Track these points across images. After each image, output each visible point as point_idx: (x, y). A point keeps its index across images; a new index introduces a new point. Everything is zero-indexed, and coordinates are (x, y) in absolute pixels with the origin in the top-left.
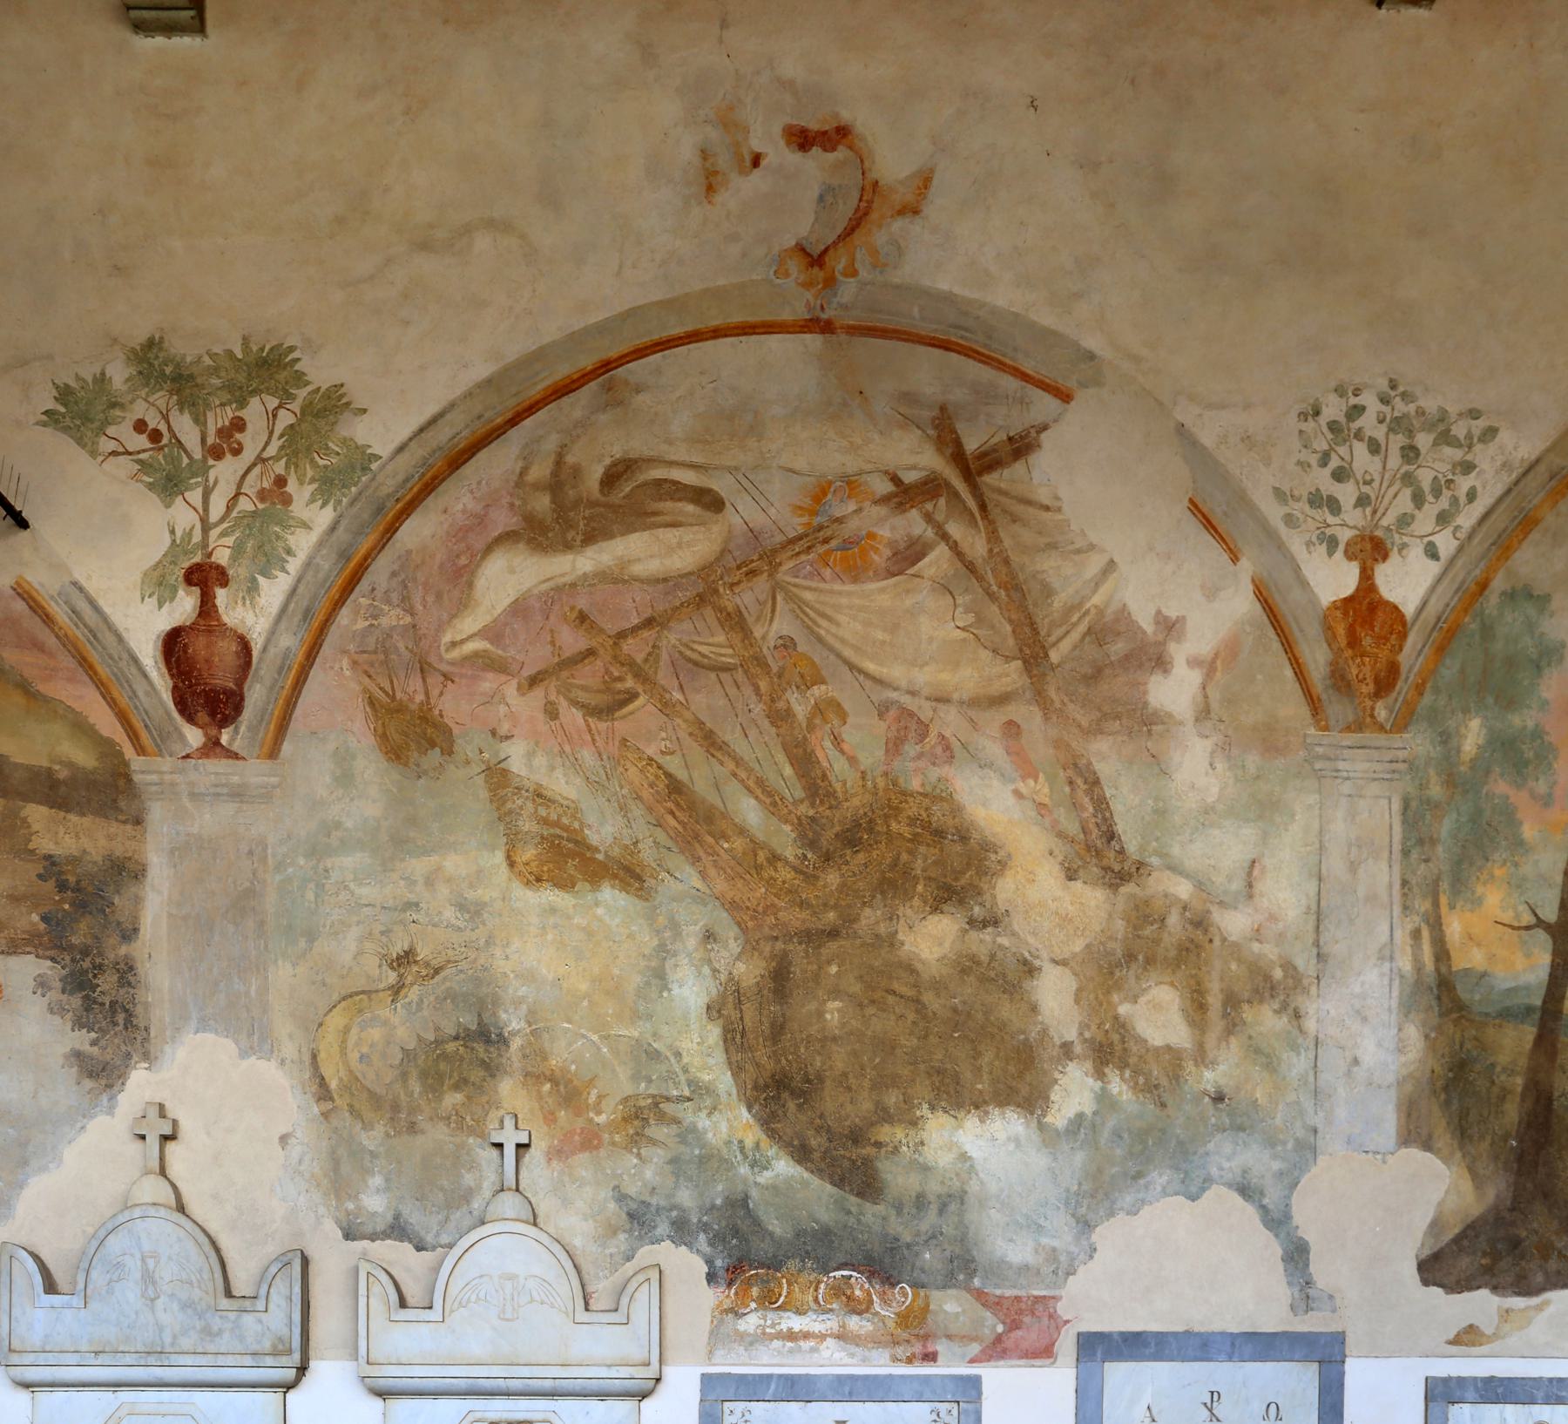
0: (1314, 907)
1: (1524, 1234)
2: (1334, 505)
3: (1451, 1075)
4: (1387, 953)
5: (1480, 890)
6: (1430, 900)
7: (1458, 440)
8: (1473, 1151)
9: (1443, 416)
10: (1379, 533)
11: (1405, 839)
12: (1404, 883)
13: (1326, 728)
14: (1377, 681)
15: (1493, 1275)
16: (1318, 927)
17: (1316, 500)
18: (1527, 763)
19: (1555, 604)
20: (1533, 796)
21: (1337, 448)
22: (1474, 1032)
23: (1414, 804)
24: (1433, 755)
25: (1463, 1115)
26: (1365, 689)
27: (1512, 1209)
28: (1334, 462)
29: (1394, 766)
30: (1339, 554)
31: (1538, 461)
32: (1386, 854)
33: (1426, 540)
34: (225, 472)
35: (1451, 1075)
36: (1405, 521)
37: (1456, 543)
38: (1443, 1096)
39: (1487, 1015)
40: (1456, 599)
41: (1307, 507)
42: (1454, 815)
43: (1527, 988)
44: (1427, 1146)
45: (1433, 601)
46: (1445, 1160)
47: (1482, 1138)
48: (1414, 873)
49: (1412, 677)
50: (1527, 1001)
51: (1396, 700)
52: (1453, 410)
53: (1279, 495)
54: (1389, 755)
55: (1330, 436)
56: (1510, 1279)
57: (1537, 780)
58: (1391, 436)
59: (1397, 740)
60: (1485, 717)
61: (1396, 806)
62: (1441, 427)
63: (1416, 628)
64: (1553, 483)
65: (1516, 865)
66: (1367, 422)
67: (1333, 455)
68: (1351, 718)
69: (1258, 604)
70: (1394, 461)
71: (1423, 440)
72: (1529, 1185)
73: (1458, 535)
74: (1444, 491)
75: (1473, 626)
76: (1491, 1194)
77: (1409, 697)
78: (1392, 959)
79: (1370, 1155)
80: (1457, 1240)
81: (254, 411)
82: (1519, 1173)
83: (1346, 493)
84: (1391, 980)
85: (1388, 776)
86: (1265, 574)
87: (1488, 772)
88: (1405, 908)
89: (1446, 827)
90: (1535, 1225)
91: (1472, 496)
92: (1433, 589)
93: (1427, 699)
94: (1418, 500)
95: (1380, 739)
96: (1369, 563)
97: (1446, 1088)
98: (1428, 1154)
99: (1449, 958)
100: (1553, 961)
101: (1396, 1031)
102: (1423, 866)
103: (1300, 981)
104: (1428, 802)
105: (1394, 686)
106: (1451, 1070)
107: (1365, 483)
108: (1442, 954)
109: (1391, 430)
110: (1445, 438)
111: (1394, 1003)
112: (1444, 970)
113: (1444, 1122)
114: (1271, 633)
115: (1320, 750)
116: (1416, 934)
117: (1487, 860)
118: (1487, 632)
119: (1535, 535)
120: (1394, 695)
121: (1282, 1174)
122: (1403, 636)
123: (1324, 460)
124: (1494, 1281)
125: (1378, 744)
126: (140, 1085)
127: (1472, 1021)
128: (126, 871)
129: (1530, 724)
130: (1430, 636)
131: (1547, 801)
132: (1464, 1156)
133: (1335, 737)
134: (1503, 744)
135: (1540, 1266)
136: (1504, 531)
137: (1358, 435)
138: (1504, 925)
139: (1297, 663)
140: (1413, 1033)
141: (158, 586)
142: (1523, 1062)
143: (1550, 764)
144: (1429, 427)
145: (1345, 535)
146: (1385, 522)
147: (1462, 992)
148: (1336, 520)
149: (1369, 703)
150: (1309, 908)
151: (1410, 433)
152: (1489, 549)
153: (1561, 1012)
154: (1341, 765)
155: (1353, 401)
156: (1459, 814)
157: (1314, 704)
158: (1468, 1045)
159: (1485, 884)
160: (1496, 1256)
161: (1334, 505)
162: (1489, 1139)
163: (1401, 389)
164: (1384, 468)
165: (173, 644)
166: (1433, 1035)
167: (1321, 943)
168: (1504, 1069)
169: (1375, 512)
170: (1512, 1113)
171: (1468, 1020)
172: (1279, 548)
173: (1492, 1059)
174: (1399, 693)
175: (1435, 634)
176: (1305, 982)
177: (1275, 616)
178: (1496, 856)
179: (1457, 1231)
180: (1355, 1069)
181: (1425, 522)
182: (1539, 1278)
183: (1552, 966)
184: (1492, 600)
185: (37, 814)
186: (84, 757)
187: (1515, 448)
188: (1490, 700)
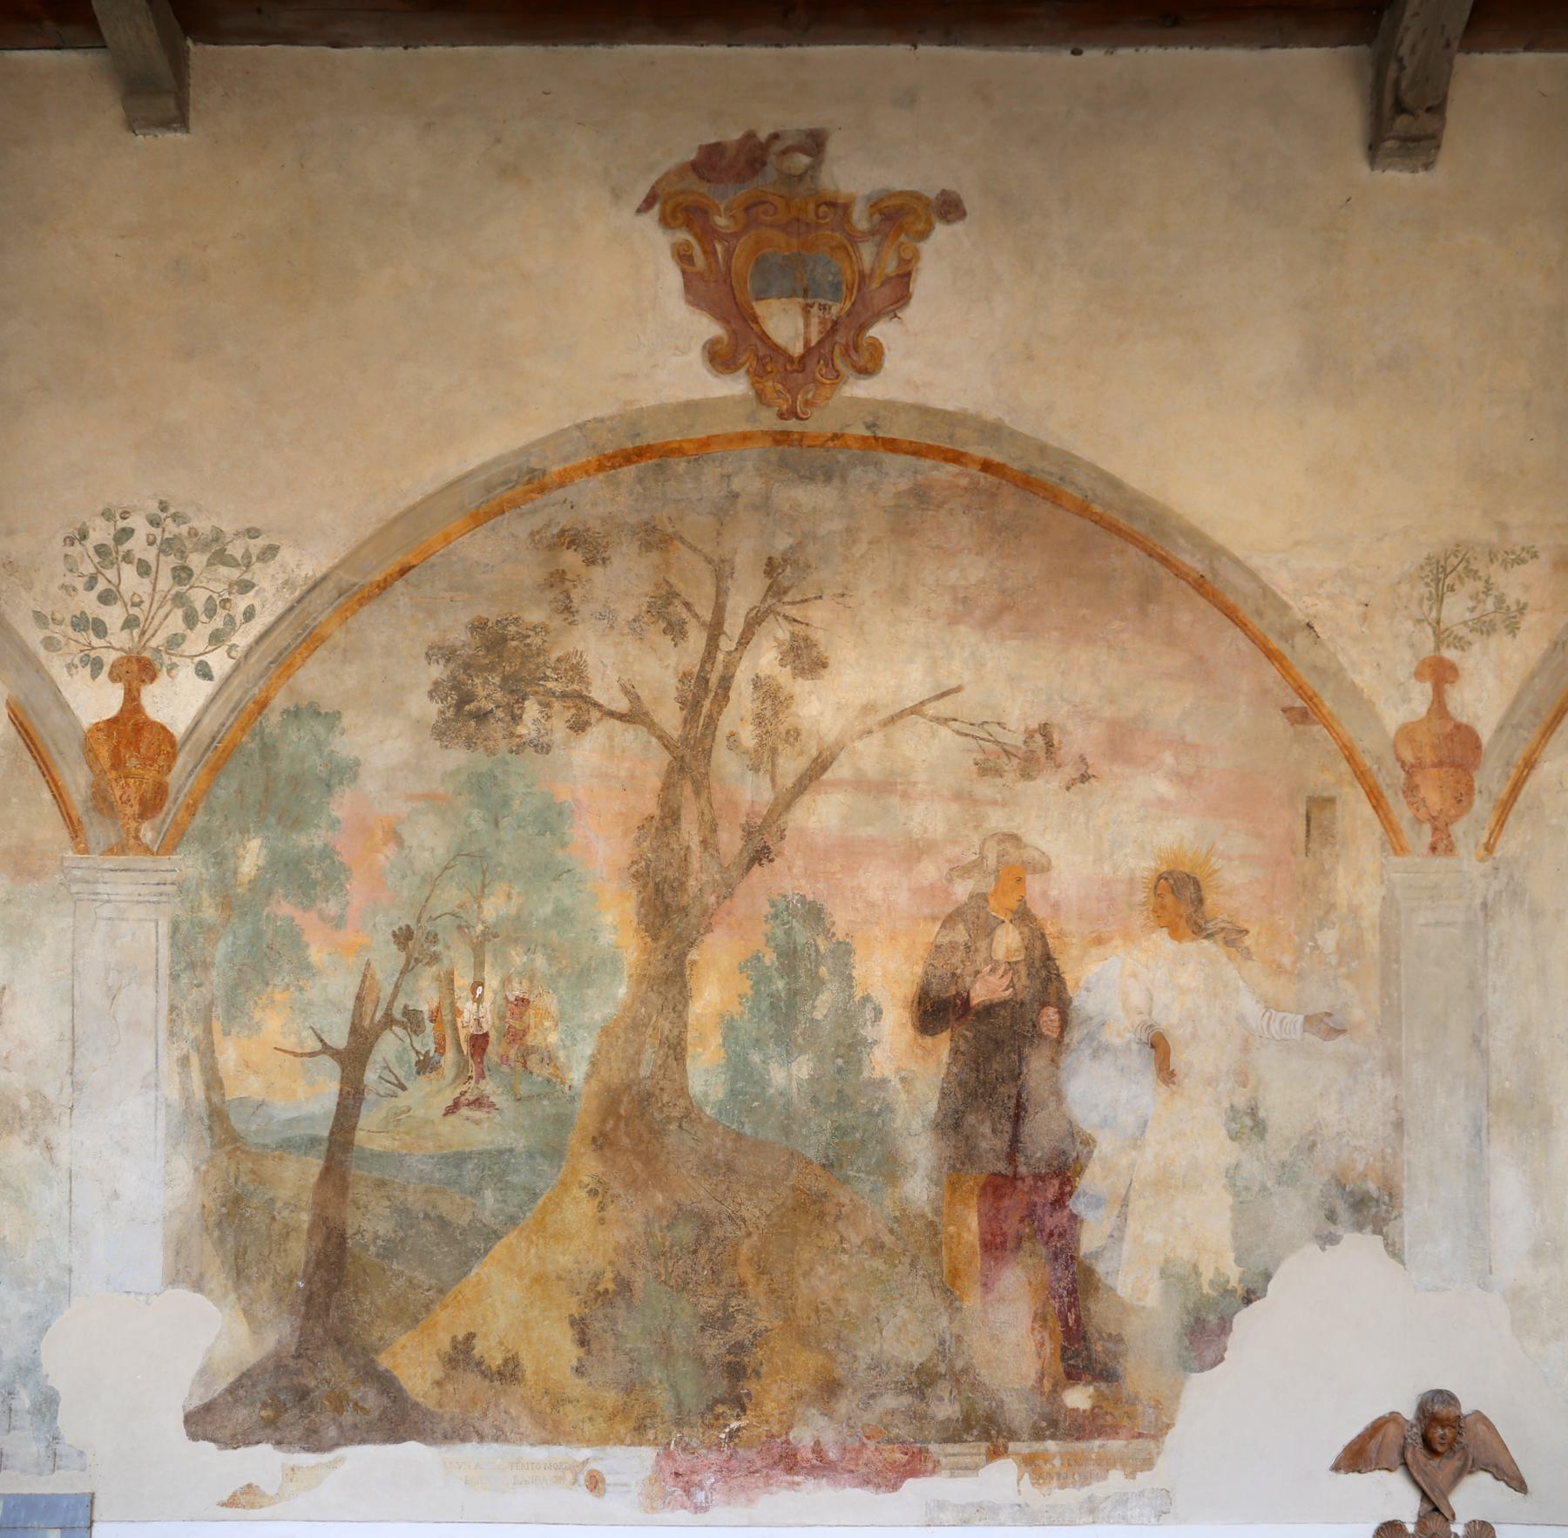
0: (68, 1034)
1: (313, 1383)
2: (100, 628)
3: (224, 1210)
5: (258, 1015)
6: (201, 1025)
7: (235, 559)
8: (251, 1292)
9: (218, 535)
10: (147, 654)
11: (173, 963)
12: (173, 1009)
13: (86, 851)
14: (142, 802)
15: (277, 1429)
16: (74, 1054)
17: (80, 622)
18: (315, 884)
19: (346, 721)
20: (323, 918)
21: (104, 571)
22: (250, 1165)
23: (184, 927)
25: (240, 1253)
26: (129, 811)
27: (299, 1356)
28: (101, 585)
29: (162, 888)
30: (103, 676)
31: (324, 578)
32: (152, 979)
33: (197, 659)
35: (224, 1210)
36: (175, 641)
37: (232, 662)
39: (265, 1146)
40: (232, 718)
41: (70, 631)
42: (231, 938)
43: (311, 1118)
44: (198, 1286)
45: (206, 720)
46: (217, 1302)
47: (262, 1278)
48: (184, 998)
50: (310, 1132)
51: (164, 821)
52: (228, 529)
53: (39, 618)
54: (157, 878)
55: (97, 559)
56: (297, 1434)
57: (327, 901)
58: (162, 557)
59: (164, 862)
60: (267, 838)
61: (165, 928)
62: (215, 547)
63: (187, 748)
64: (342, 599)
65: (301, 989)
66: (137, 545)
67: (100, 578)
68: (113, 839)
69: (12, 728)
70: (165, 581)
71: (197, 561)
72: (319, 1331)
73: (233, 654)
74: (219, 610)
75: (252, 745)
76: (270, 1341)
77: (179, 817)
79: (132, 1295)
80: (232, 1390)
82: (307, 1316)
83: (113, 616)
85: (155, 899)
87: (270, 894)
88: (172, 1034)
89: (221, 950)
90: (326, 1374)
91: (249, 614)
92: (206, 709)
93: (200, 819)
94: (191, 620)
95: (146, 862)
96: (135, 684)
97: (219, 1224)
98: (198, 1295)
99: (221, 1087)
100: (341, 1090)
101: (163, 1164)
102: (195, 990)
104: (201, 924)
105: (162, 808)
106: (224, 1205)
107: (134, 605)
108: (213, 1081)
109: (161, 551)
110: (221, 557)
111: (161, 1134)
112: (215, 1099)
113: (218, 1261)
114: (27, 756)
115: (78, 873)
116: (184, 1061)
117: (267, 984)
118: (268, 751)
119: (321, 652)
120: (162, 815)
121: (30, 1317)
122: (173, 757)
123: (91, 583)
124: (278, 1436)
125: (144, 866)
127: (247, 1153)
129: (318, 844)
130: (203, 756)
131: (338, 923)
132: (239, 1299)
133: (95, 859)
134: (286, 865)
135: (334, 1419)
136: (286, 649)
137: (127, 557)
138: (285, 1051)
139: (56, 785)
140: (183, 1167)
142: (307, 1197)
143: (341, 885)
144: (203, 547)
145: (110, 657)
146: (153, 644)
147: (236, 1122)
148: (102, 643)
149: (133, 825)
150: (62, 1034)
151: (183, 554)
152: (268, 668)
153: (352, 1143)
154: (101, 888)
155: (121, 524)
156: (235, 937)
157: (74, 827)
158: (244, 1179)
159: (263, 1009)
160: (280, 1408)
162: (270, 1280)
163: (172, 510)
164: (154, 590)
166: (204, 1168)
167: (76, 1070)
168: (286, 1205)
169: (143, 633)
170: (298, 1252)
171: (243, 1152)
172: (37, 672)
173: (271, 1194)
175: (209, 754)
176: (56, 1112)
178: (278, 980)
179: (231, 1379)
181: (197, 641)
182: (333, 1432)
183: (341, 1095)
184: (273, 718)
187: (298, 566)
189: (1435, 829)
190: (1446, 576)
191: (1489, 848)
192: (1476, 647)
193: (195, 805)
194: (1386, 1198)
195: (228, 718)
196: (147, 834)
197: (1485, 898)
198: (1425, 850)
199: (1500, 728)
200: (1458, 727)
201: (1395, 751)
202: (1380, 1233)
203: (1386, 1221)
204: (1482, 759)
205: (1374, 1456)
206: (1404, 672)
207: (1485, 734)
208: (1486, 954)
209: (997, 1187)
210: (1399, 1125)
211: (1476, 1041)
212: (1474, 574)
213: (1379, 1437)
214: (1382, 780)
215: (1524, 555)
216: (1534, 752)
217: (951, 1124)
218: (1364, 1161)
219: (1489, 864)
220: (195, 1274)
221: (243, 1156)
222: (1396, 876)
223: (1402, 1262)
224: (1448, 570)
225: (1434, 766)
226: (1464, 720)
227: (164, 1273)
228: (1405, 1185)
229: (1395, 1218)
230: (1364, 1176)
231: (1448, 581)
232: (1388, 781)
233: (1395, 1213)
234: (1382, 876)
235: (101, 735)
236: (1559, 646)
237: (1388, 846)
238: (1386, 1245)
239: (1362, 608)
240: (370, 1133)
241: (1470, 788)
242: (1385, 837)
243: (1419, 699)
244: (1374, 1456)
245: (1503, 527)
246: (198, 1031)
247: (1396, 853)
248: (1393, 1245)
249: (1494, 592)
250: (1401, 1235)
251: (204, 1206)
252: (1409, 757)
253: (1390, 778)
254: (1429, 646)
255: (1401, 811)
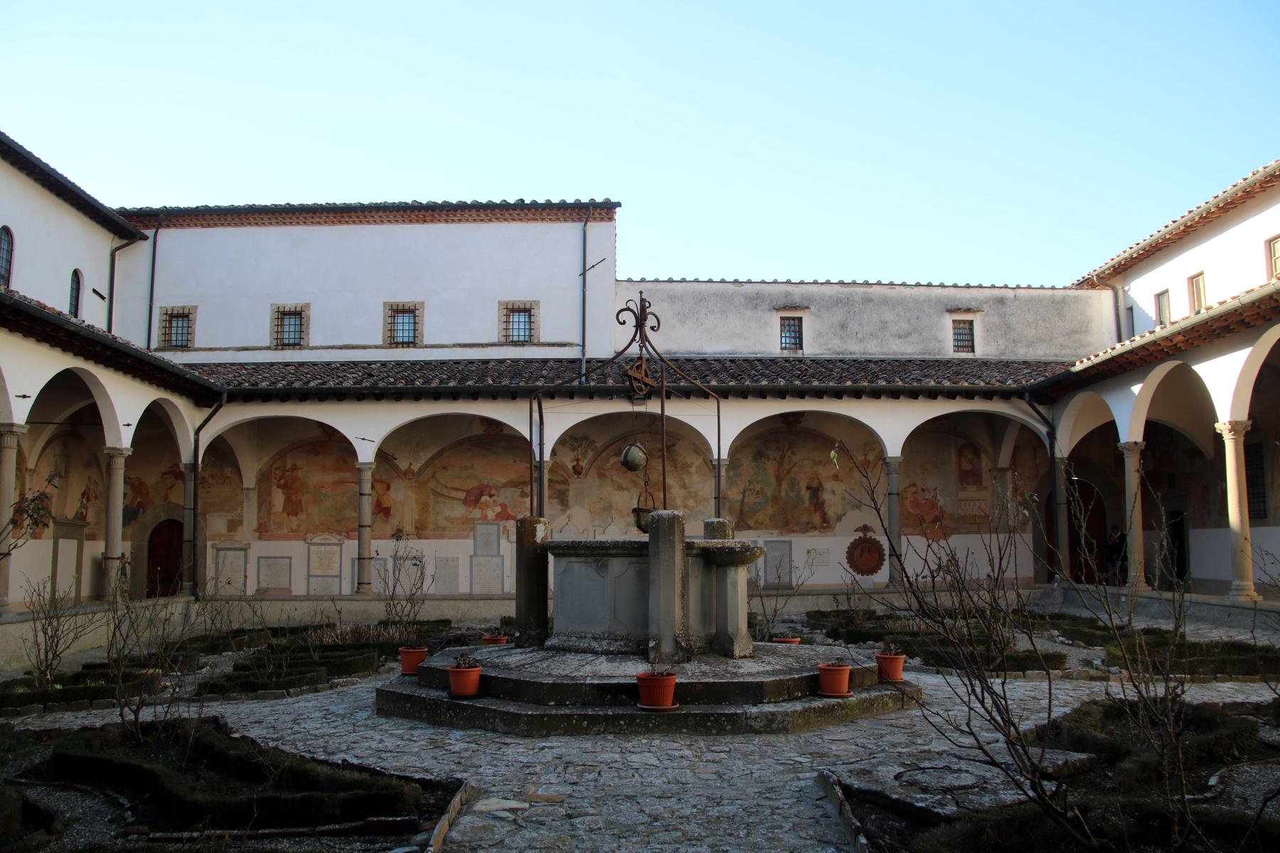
34: (580, 449)
81: (584, 442)
126: (568, 512)
128: (567, 490)
141: (572, 461)
165: (573, 467)
170: (738, 512)
185: (557, 485)
186: (562, 479)
209: (815, 505)
217: (810, 499)
240: (746, 500)
243: (863, 458)
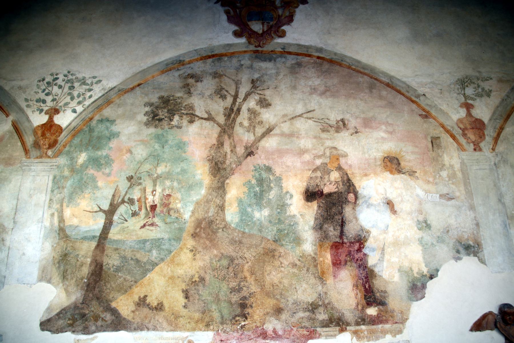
0: (15, 207)
2: (44, 102)
4: (41, 221)
5: (79, 201)
6: (60, 204)
7: (88, 84)
8: (67, 283)
9: (84, 78)
10: (57, 107)
11: (53, 187)
12: (51, 200)
13: (29, 158)
16: (16, 213)
17: (38, 101)
18: (102, 165)
19: (117, 122)
20: (103, 173)
21: (48, 88)
22: (71, 244)
23: (57, 177)
24: (67, 163)
25: (65, 271)
26: (45, 147)
28: (47, 91)
29: (52, 167)
30: (43, 113)
31: (115, 87)
32: (45, 192)
33: (72, 108)
35: (61, 258)
36: (66, 104)
37: (83, 109)
38: (57, 265)
39: (77, 239)
41: (35, 103)
42: (72, 180)
43: (94, 230)
44: (49, 281)
45: (73, 123)
46: (55, 286)
47: (72, 279)
48: (55, 197)
49: (62, 143)
50: (93, 234)
51: (55, 149)
52: (87, 76)
53: (26, 100)
54: (51, 164)
55: (46, 85)
57: (106, 169)
58: (66, 84)
59: (54, 160)
61: (51, 178)
62: (83, 81)
63: (66, 130)
64: (119, 92)
65: (94, 194)
66: (59, 82)
68: (39, 154)
70: (66, 90)
71: (76, 85)
73: (84, 106)
74: (81, 96)
75: (87, 129)
76: (73, 299)
77: (60, 148)
78: (42, 222)
80: (58, 314)
83: (49, 99)
84: (41, 229)
85: (49, 170)
86: (17, 119)
87: (87, 167)
88: (49, 207)
89: (69, 183)
91: (90, 97)
92: (73, 120)
93: (67, 149)
94: (72, 99)
95: (48, 160)
96: (52, 115)
97: (59, 263)
98: (49, 285)
99: (64, 221)
100: (105, 222)
101: (41, 244)
103: (5, 230)
104: (63, 177)
105: (55, 146)
106: (61, 257)
107: (55, 95)
108: (62, 220)
111: (42, 236)
113: (57, 274)
114: (15, 134)
115: (26, 164)
116: (53, 215)
117: (83, 192)
118: (91, 130)
119: (112, 105)
120: (55, 148)
122: (61, 133)
125: (47, 161)
127: (71, 241)
129: (104, 154)
131: (109, 175)
132: (63, 285)
133: (32, 160)
134: (93, 160)
136: (101, 105)
138: (87, 211)
140: (48, 246)
142: (90, 254)
143: (111, 165)
145: (45, 109)
147: (68, 232)
148: (44, 105)
149: (45, 150)
150: (13, 208)
151: (73, 83)
152: (94, 109)
153: (107, 237)
154: (32, 167)
155: (55, 76)
156: (74, 180)
158: (69, 249)
159: (81, 199)
161: (44, 102)
162: (75, 279)
166: (55, 245)
167: (16, 218)
168: (83, 256)
169: (57, 102)
170: (86, 271)
171: (69, 241)
173: (78, 253)
174: (57, 148)
175: (73, 132)
176: (7, 230)
177: (17, 130)
178: (87, 191)
179: (58, 311)
180: (23, 256)
181: (73, 104)
183: (105, 223)
184: (94, 123)
187: (107, 85)
188: (90, 148)
189: (474, 145)
190: (465, 83)
191: (493, 149)
192: (478, 100)
193: (66, 145)
194: (477, 246)
195: (80, 122)
196: (50, 153)
197: (495, 162)
198: (472, 150)
199: (490, 120)
200: (477, 119)
201: (457, 125)
202: (476, 256)
203: (478, 253)
204: (486, 127)
205: (485, 326)
206: (456, 106)
207: (486, 121)
208: (498, 177)
209: (336, 246)
210: (477, 225)
211: (500, 200)
212: (474, 83)
213: (486, 320)
214: (454, 132)
215: (488, 79)
216: (503, 125)
217: (319, 227)
218: (467, 235)
219: (494, 153)
220: (48, 277)
221: (69, 242)
222: (464, 157)
223: (486, 265)
224: (465, 82)
225: (471, 129)
226: (478, 118)
227: (38, 277)
228: (483, 242)
229: (481, 252)
230: (468, 239)
231: (465, 84)
232: (457, 133)
233: (481, 250)
234: (459, 157)
235: (40, 128)
236: (504, 100)
237: (460, 149)
238: (479, 260)
239: (440, 91)
240: (114, 234)
241: (484, 134)
242: (458, 147)
244: (485, 326)
245: (479, 72)
246: (58, 206)
247: (462, 151)
248: (482, 259)
249: (481, 87)
250: (484, 256)
251: (54, 257)
252: (462, 126)
253: (457, 132)
254: (463, 100)
255: (463, 141)
